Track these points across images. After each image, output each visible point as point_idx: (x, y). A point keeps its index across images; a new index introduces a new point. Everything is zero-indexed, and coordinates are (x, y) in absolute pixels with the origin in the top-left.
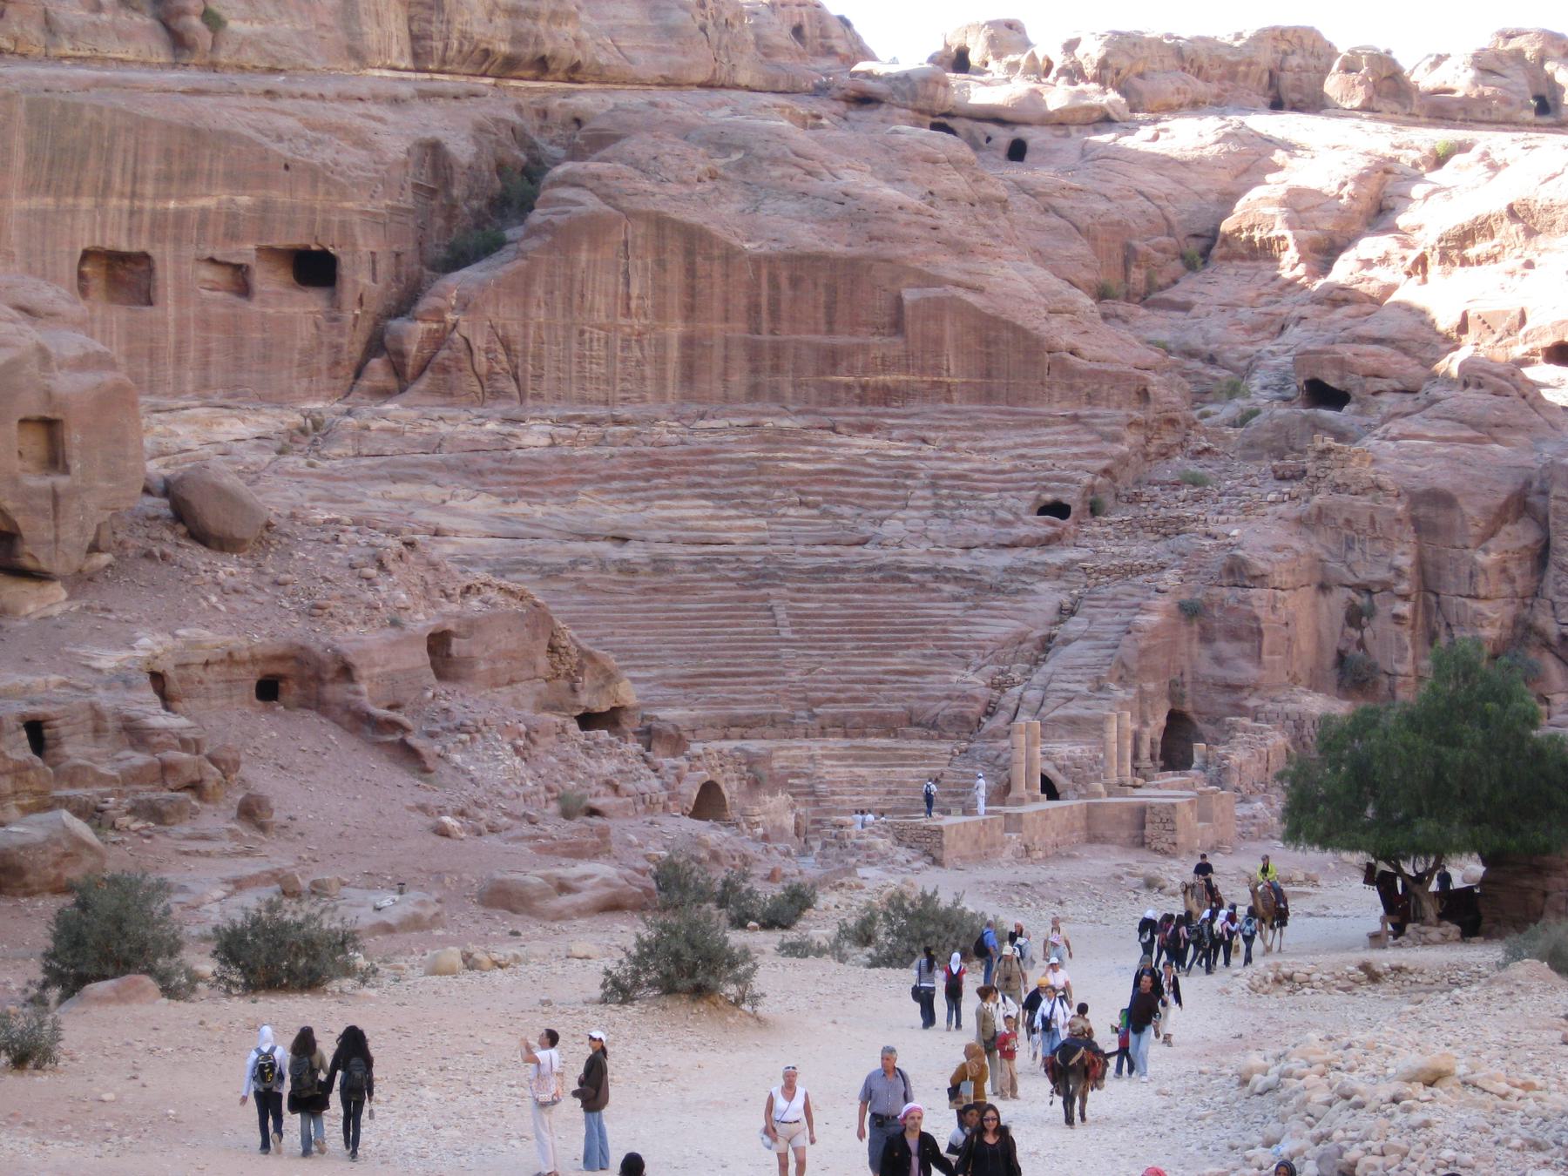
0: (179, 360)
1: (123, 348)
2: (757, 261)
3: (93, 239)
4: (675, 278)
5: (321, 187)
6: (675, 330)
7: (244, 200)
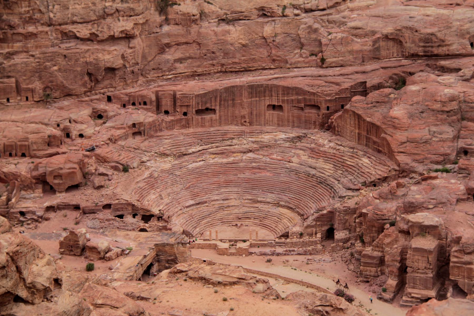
0: (288, 122)
2: (368, 122)
4: (357, 122)
5: (316, 96)
6: (357, 131)
7: (300, 97)
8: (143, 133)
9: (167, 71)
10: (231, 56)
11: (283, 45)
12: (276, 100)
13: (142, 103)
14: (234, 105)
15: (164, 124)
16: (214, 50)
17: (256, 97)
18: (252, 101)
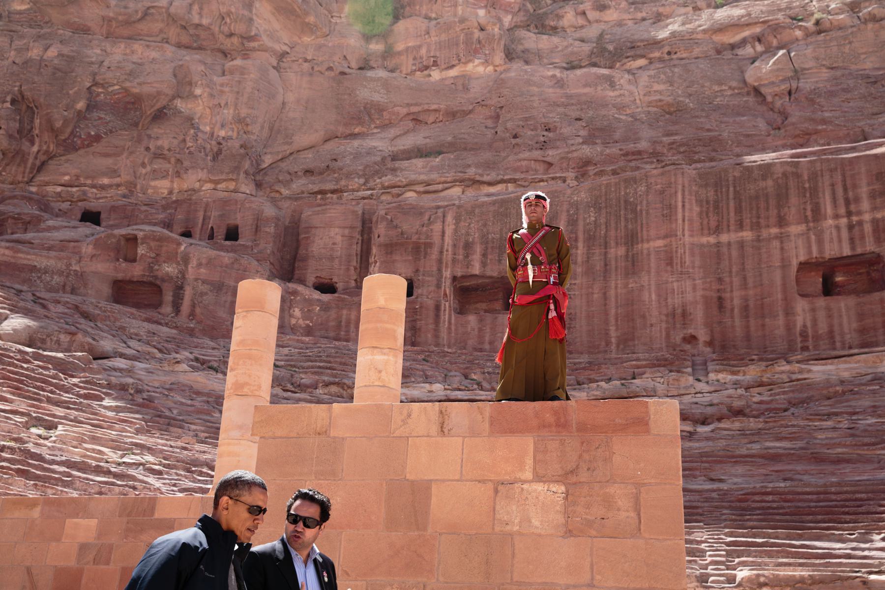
1: (855, 325)
3: (810, 252)
8: (168, 297)
9: (360, 177)
10: (617, 135)
11: (831, 94)
12: (845, 234)
13: (220, 234)
14: (633, 265)
15: (297, 312)
16: (554, 117)
17: (741, 226)
18: (718, 245)
